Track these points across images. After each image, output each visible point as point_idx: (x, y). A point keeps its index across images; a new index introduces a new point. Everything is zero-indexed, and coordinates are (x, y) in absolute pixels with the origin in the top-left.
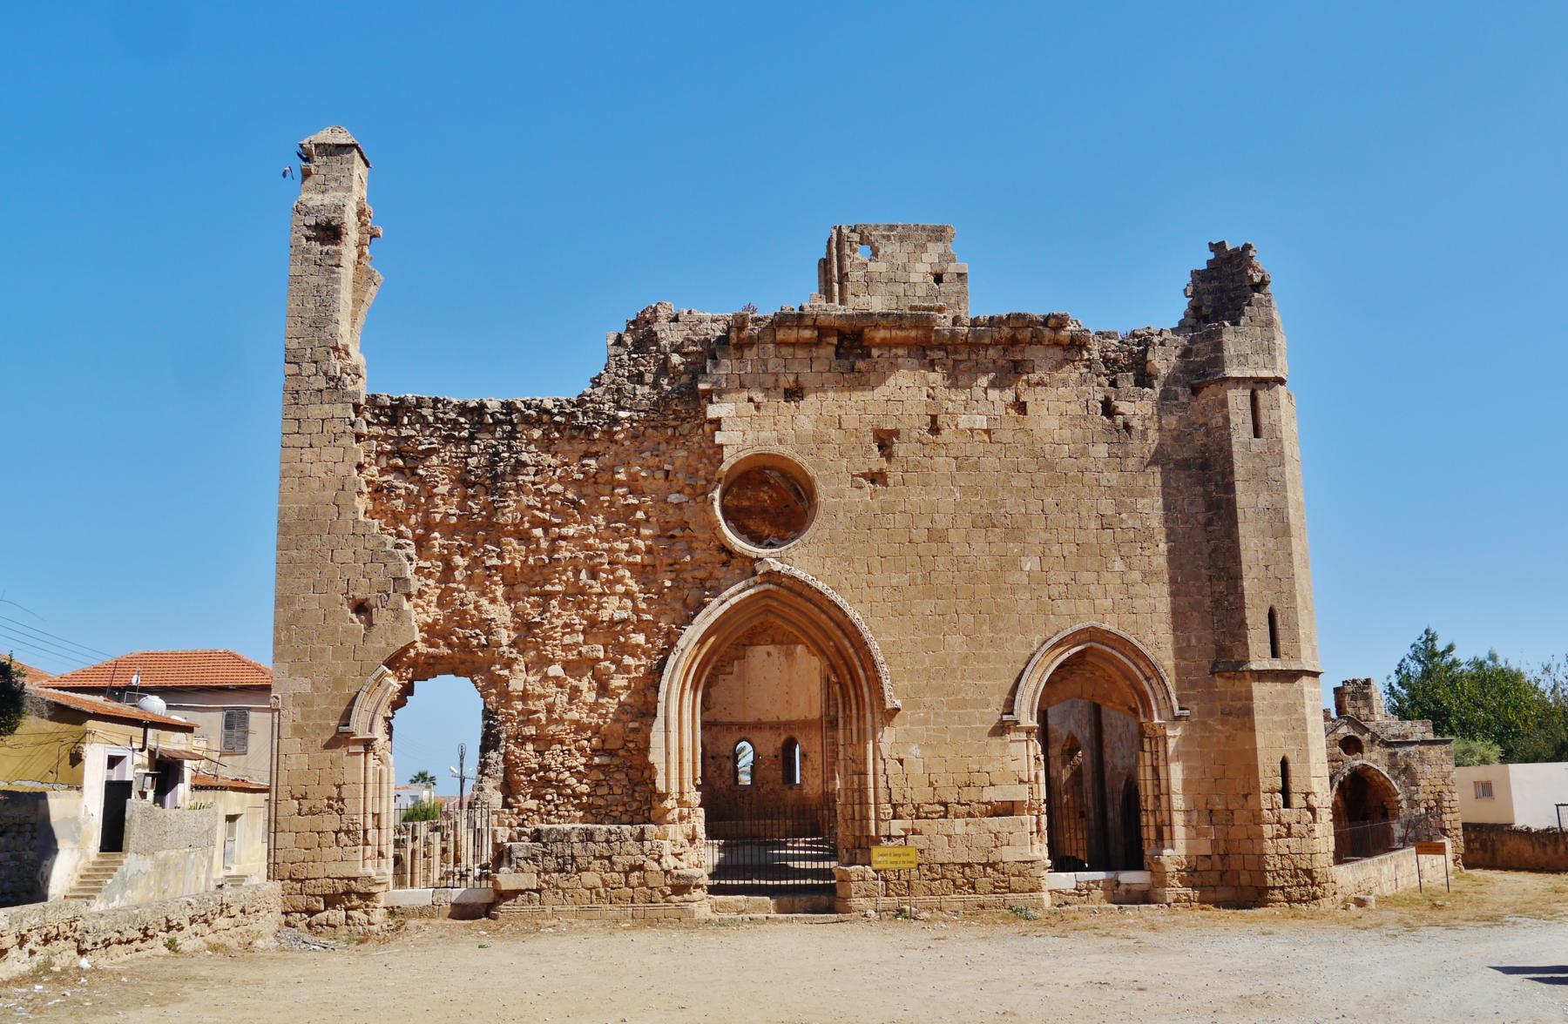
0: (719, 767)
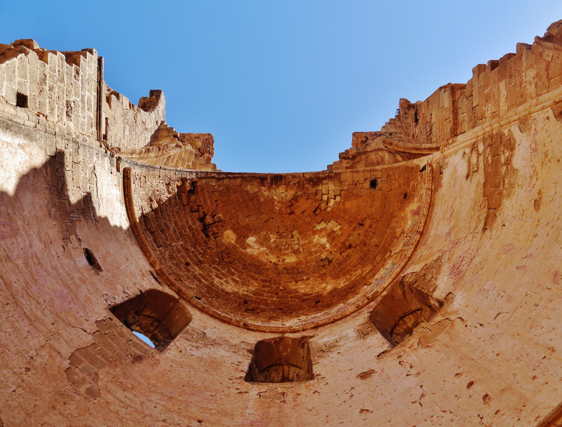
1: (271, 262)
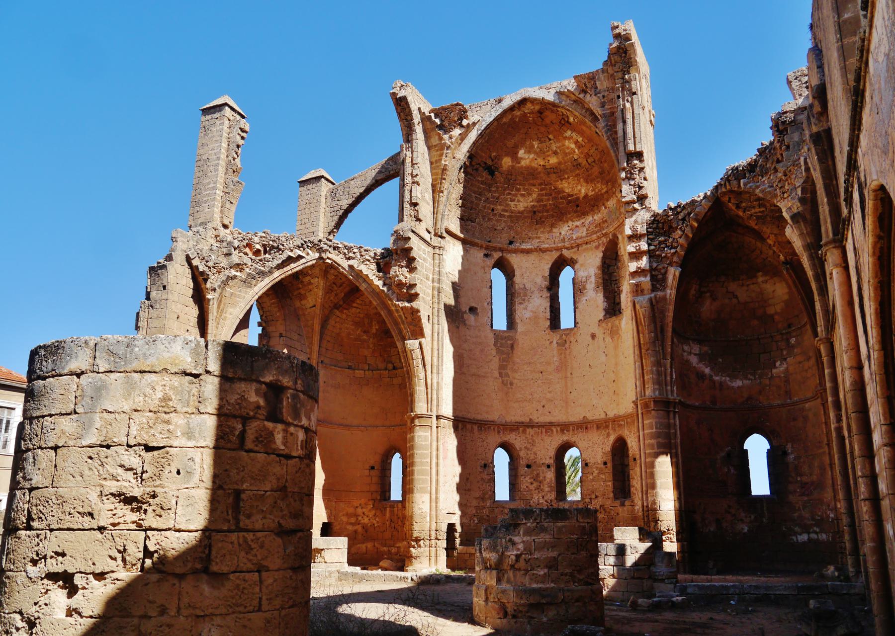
0: (536, 478)
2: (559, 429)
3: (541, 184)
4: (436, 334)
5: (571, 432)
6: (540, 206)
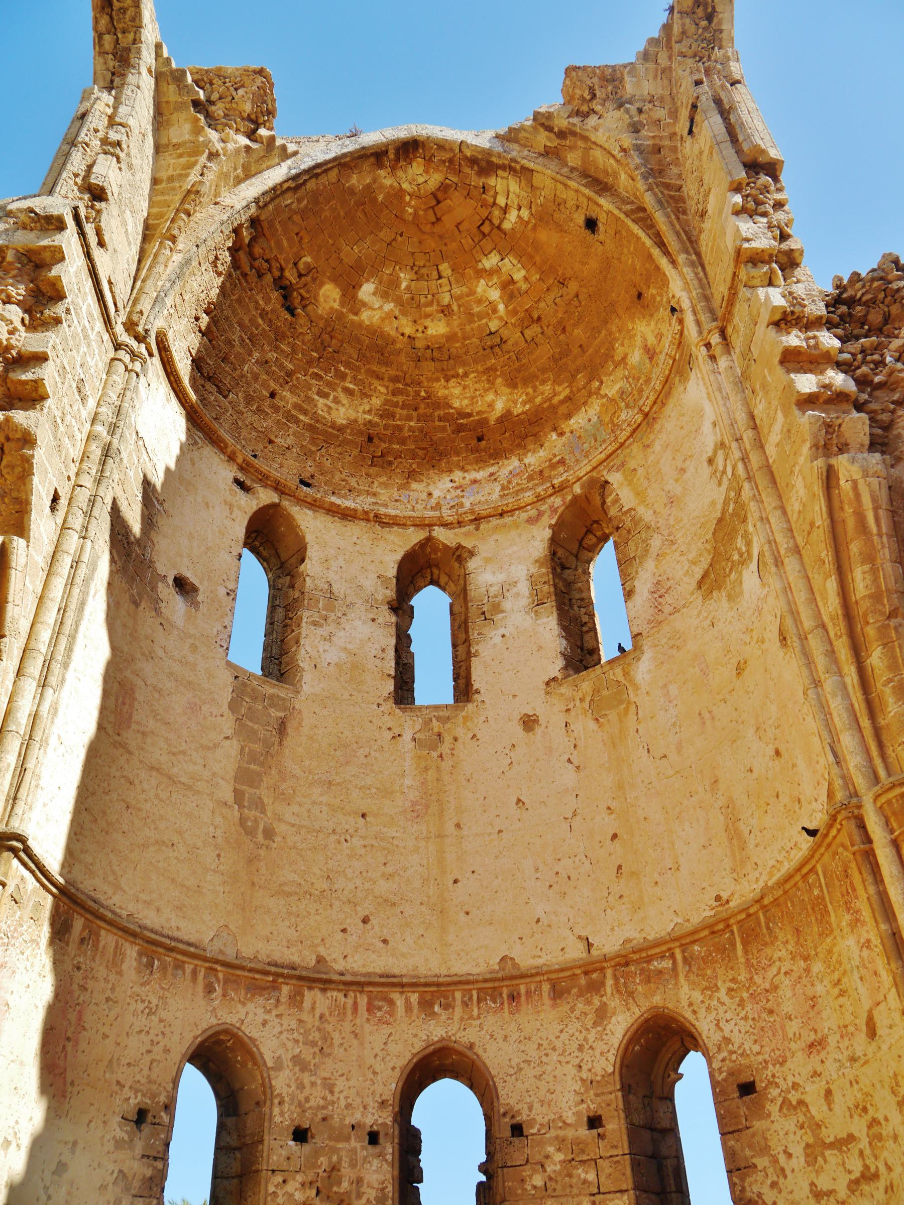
1: (403, 335)
2: (414, 998)
3: (395, 379)
4: (66, 561)
5: (458, 1011)
6: (386, 427)
